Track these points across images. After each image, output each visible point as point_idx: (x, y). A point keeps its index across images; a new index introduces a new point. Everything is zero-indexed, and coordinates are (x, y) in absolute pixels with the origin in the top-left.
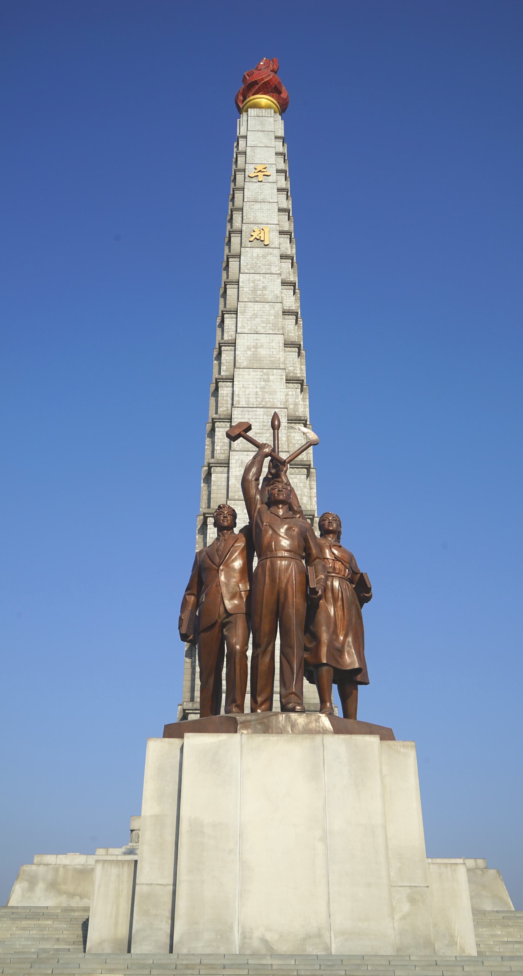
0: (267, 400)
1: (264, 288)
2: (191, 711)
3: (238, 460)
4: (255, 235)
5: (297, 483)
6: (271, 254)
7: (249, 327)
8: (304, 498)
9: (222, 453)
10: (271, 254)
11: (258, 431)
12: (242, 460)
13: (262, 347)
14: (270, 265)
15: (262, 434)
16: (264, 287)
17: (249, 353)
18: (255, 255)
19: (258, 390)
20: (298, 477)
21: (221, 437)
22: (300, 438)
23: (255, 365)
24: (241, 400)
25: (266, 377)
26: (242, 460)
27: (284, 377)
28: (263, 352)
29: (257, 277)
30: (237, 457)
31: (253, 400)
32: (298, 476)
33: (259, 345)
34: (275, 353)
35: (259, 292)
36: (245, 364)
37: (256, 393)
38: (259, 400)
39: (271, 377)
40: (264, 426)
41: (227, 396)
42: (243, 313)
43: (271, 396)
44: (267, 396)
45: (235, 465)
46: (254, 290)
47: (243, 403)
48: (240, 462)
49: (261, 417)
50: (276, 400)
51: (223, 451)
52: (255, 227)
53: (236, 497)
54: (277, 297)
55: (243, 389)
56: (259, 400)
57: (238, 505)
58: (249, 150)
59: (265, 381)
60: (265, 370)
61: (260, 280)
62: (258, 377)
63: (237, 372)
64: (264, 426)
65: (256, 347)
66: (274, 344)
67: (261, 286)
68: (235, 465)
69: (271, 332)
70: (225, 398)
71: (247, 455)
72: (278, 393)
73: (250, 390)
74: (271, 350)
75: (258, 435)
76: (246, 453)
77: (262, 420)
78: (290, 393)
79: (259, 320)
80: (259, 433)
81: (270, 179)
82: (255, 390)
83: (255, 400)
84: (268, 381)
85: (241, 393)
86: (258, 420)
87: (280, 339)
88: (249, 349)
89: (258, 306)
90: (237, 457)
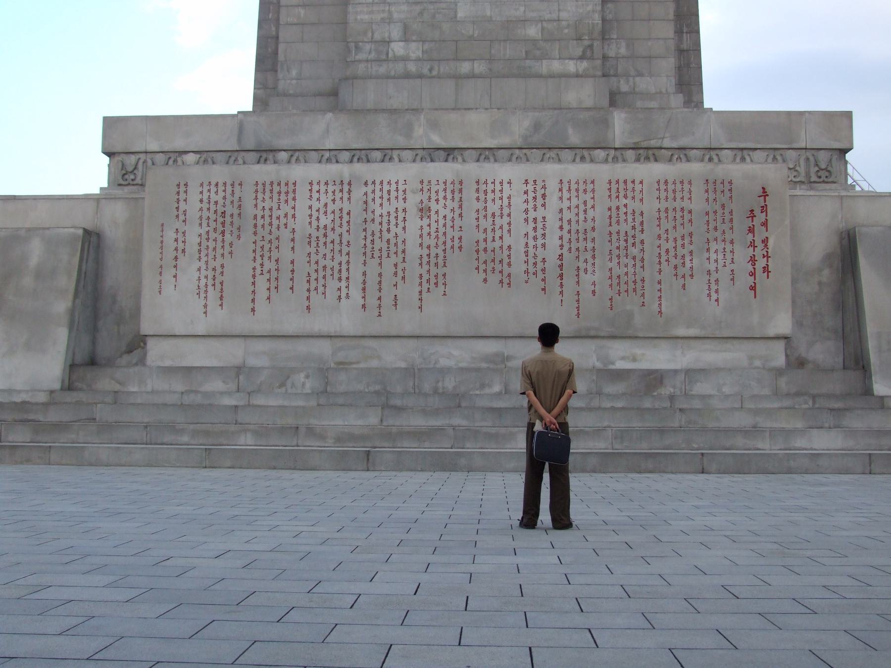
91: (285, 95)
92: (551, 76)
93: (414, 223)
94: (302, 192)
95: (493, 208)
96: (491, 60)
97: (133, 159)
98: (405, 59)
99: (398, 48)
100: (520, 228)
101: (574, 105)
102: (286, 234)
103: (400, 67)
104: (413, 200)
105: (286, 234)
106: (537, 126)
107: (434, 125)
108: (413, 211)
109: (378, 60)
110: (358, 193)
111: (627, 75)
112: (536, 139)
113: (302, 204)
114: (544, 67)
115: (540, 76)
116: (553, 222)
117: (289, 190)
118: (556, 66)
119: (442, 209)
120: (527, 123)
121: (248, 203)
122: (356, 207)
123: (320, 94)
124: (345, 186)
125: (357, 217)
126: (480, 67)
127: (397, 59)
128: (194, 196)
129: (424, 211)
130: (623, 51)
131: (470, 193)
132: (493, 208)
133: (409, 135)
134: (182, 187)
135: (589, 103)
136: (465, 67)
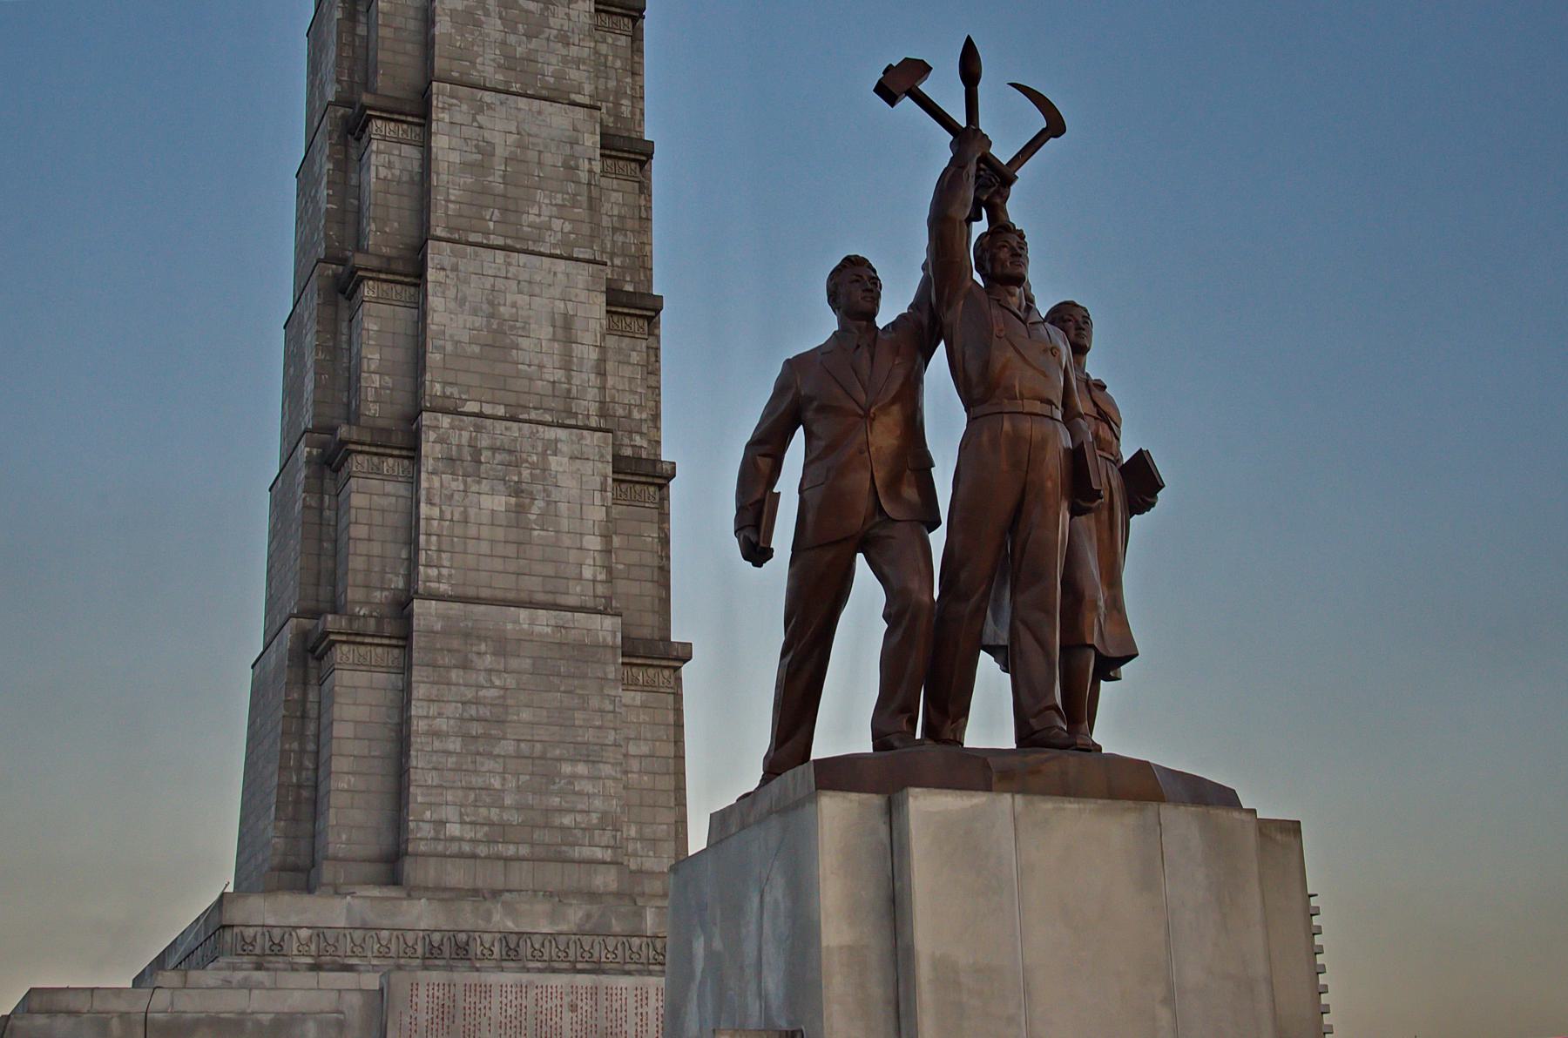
2: (344, 638)
5: (606, 56)
15: (945, 89)
20: (610, 40)
53: (455, 74)
91: (336, 859)
92: (581, 862)
93: (567, 1015)
94: (496, 991)
95: (616, 1005)
96: (532, 845)
97: (251, 931)
98: (461, 839)
99: (454, 829)
100: (632, 1019)
101: (602, 890)
102: (485, 1021)
103: (454, 848)
104: (567, 1000)
105: (485, 1021)
106: (589, 916)
107: (510, 910)
108: (566, 1008)
109: (436, 839)
110: (532, 993)
111: (635, 854)
112: (587, 927)
113: (495, 1001)
114: (576, 853)
115: (573, 861)
116: (652, 1016)
117: (487, 990)
118: (587, 852)
119: (585, 1006)
120: (580, 914)
121: (460, 998)
122: (530, 1002)
123: (371, 861)
124: (522, 988)
125: (531, 1009)
126: (524, 850)
127: (453, 839)
128: (422, 992)
129: (573, 1008)
130: (633, 833)
131: (602, 996)
132: (616, 1005)
133: (488, 919)
134: (415, 986)
135: (613, 887)
136: (511, 850)
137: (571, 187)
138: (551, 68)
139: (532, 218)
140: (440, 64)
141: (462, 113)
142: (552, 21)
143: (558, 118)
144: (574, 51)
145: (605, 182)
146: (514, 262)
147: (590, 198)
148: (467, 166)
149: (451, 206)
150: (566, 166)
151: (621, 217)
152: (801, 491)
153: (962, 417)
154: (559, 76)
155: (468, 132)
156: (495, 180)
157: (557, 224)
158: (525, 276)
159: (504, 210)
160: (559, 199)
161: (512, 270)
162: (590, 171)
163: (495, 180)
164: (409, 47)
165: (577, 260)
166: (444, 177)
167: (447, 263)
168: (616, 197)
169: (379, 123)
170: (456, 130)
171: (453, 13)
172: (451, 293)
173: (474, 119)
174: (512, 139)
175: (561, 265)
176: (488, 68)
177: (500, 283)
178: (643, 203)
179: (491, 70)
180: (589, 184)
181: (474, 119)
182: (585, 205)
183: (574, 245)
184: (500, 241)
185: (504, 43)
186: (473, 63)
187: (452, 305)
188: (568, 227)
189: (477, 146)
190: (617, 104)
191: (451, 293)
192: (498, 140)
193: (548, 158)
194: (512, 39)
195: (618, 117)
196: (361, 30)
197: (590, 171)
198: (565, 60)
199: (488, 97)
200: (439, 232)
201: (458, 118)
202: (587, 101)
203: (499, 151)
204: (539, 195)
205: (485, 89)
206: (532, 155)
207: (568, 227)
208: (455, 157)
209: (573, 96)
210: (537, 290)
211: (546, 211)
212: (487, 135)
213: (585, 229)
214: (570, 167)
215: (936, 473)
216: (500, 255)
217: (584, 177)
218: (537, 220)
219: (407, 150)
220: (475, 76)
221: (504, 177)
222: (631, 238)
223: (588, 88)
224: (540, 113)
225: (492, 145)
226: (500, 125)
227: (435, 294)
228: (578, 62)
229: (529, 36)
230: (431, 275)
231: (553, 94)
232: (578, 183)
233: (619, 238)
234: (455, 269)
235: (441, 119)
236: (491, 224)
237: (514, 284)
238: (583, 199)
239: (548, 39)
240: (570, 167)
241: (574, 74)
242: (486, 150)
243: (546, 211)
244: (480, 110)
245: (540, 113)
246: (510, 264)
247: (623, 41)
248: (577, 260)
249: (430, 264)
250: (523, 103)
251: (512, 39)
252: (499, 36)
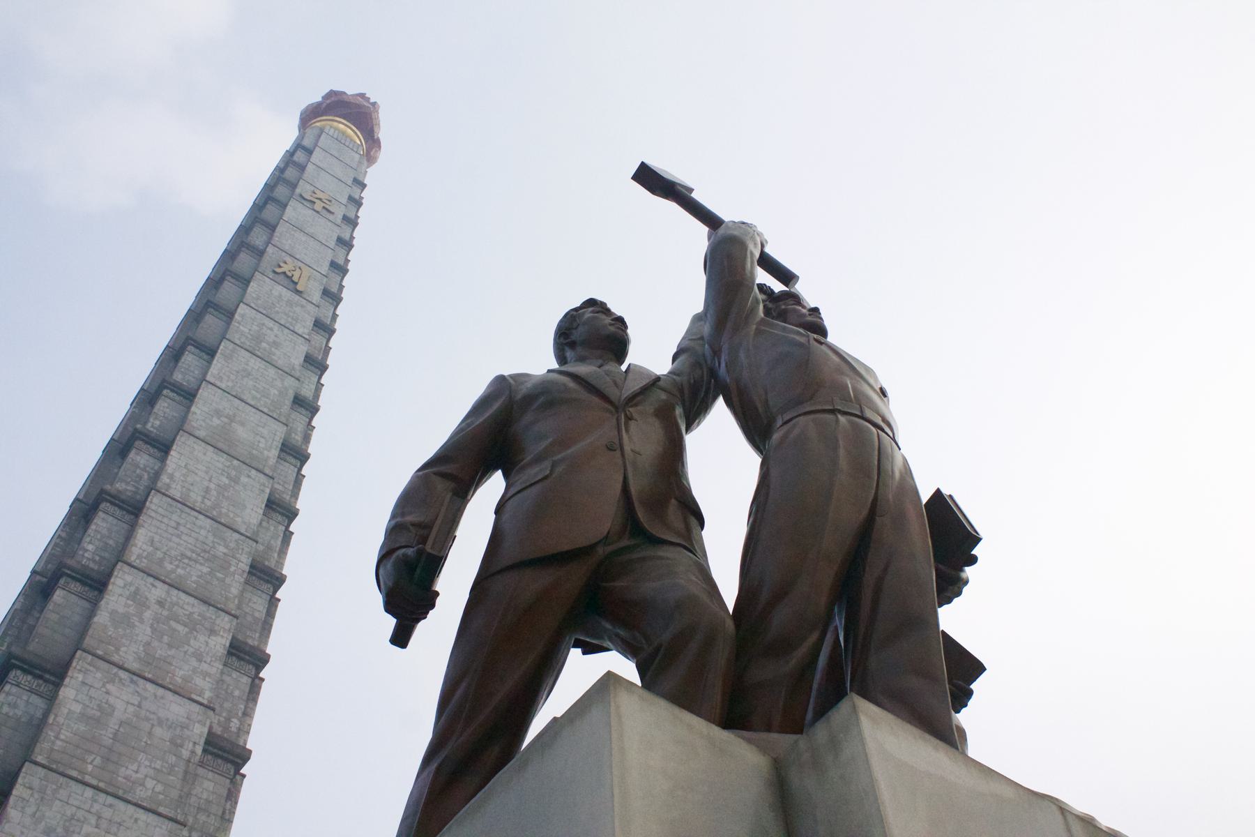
0: (224, 511)
1: (276, 344)
3: (131, 584)
4: (285, 268)
6: (302, 306)
7: (230, 384)
8: (235, 720)
9: (94, 561)
10: (302, 306)
11: (189, 554)
12: (138, 589)
13: (242, 424)
14: (296, 320)
16: (274, 342)
17: (216, 421)
18: (275, 293)
19: (212, 486)
21: (105, 532)
22: (261, 608)
23: (221, 444)
24: (174, 486)
25: (233, 473)
26: (138, 589)
27: (268, 491)
28: (241, 433)
29: (271, 324)
30: (129, 578)
31: (195, 497)
32: (235, 674)
33: (238, 419)
34: (261, 445)
35: (264, 345)
36: (202, 434)
37: (207, 490)
38: (209, 503)
39: (244, 479)
40: (205, 551)
41: (144, 470)
42: (228, 358)
43: (231, 508)
44: (225, 504)
45: (119, 591)
46: (258, 338)
47: (176, 492)
48: (132, 589)
49: (203, 532)
50: (239, 519)
51: (97, 558)
52: (288, 259)
53: (100, 652)
54: (294, 369)
55: (184, 471)
56: (209, 503)
57: (98, 669)
58: (310, 167)
59: (229, 477)
60: (235, 462)
61: (271, 329)
62: (220, 466)
63: (181, 439)
64: (205, 551)
65: (232, 419)
66: (265, 432)
67: (271, 338)
68: (119, 591)
69: (265, 410)
70: (138, 471)
71: (153, 585)
72: (248, 511)
73: (198, 479)
74: (258, 438)
75: (186, 561)
76: (151, 580)
77: (201, 538)
78: (264, 524)
79: (251, 383)
80: (190, 559)
81: (331, 217)
82: (206, 483)
83: (199, 499)
84: (236, 480)
85: (177, 474)
86: (193, 534)
87: (280, 432)
88: (218, 413)
89: (255, 364)
90: (129, 578)
137: (172, 759)
138: (182, 673)
139: (129, 772)
140: (88, 642)
141: (95, 678)
142: (192, 642)
143: (177, 709)
144: (205, 667)
145: (201, 771)
146: (101, 800)
147: (186, 772)
148: (83, 717)
149: (59, 743)
150: (172, 741)
151: (208, 801)
152: (498, 511)
153: (752, 461)
154: (186, 679)
155: (93, 692)
156: (106, 736)
157: (150, 783)
158: (107, 813)
159: (107, 759)
160: (158, 764)
161: (96, 807)
162: (193, 752)
163: (106, 736)
164: (67, 631)
165: (159, 814)
166: (61, 720)
167: (36, 783)
168: (209, 785)
169: (19, 672)
170: (85, 689)
171: (113, 613)
172: (30, 810)
173: (104, 686)
174: (131, 709)
175: (143, 816)
176: (129, 654)
177: (80, 814)
178: (228, 806)
179: (131, 658)
180: (189, 761)
181: (104, 686)
182: (180, 776)
183: (160, 804)
184: (94, 782)
185: (148, 644)
186: (118, 649)
187: (28, 821)
188: (159, 788)
189: (99, 706)
190: (228, 720)
191: (30, 810)
192: (120, 706)
193: (158, 731)
194: (155, 644)
195: (226, 728)
196: (31, 621)
197: (193, 752)
198: (194, 670)
199: (122, 674)
200: (39, 759)
201: (89, 680)
202: (205, 702)
203: (118, 714)
204: (142, 756)
205: (121, 668)
206: (146, 726)
207: (159, 788)
208: (77, 708)
209: (194, 697)
210: (114, 829)
211: (143, 771)
212: (112, 700)
213: (175, 794)
214: (176, 744)
215: (710, 536)
216: (89, 792)
217: (185, 754)
218: (134, 775)
219: (36, 700)
220: (116, 658)
221: (115, 734)
222: (212, 820)
223: (208, 694)
224: (162, 698)
225: (113, 708)
226: (125, 698)
227: (15, 807)
228: (205, 675)
229: (170, 646)
230: (18, 790)
231: (178, 690)
232: (179, 756)
233: (202, 818)
234: (42, 791)
235: (75, 677)
236: (90, 768)
237: (93, 821)
238: (180, 770)
239: (185, 652)
240: (176, 744)
241: (199, 681)
242: (106, 711)
243: (143, 771)
244: (112, 681)
245: (162, 698)
246: (96, 801)
247: (245, 680)
248: (159, 814)
249: (20, 780)
250: (150, 686)
251: (155, 644)
252: (146, 639)
